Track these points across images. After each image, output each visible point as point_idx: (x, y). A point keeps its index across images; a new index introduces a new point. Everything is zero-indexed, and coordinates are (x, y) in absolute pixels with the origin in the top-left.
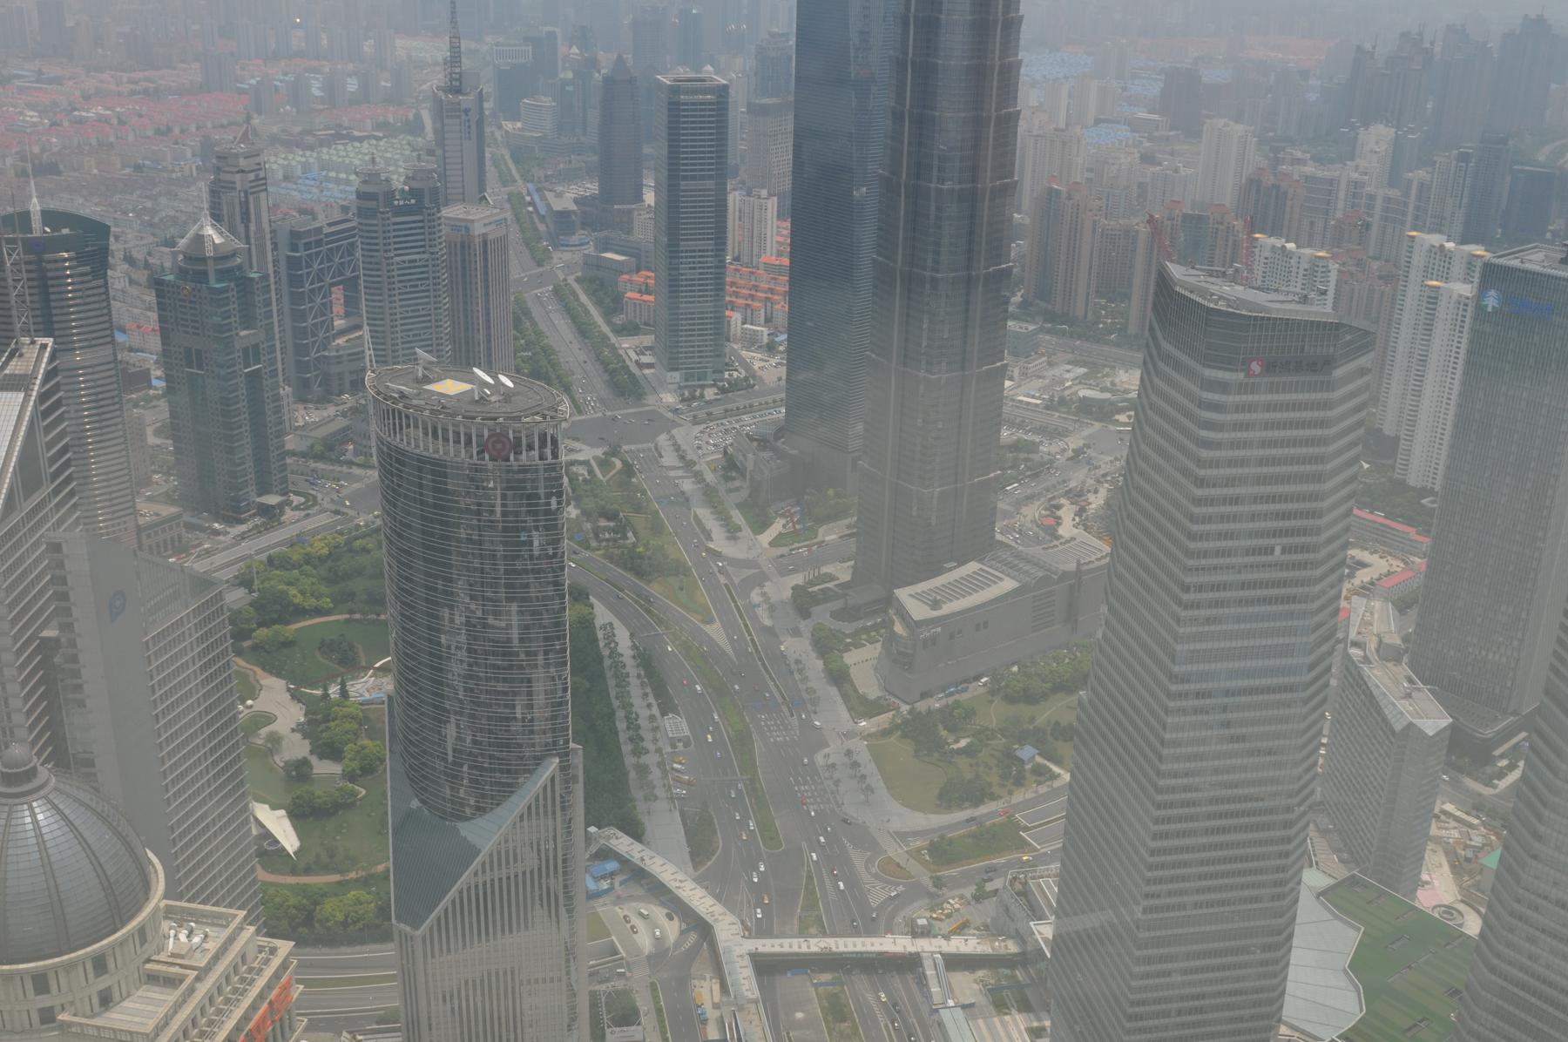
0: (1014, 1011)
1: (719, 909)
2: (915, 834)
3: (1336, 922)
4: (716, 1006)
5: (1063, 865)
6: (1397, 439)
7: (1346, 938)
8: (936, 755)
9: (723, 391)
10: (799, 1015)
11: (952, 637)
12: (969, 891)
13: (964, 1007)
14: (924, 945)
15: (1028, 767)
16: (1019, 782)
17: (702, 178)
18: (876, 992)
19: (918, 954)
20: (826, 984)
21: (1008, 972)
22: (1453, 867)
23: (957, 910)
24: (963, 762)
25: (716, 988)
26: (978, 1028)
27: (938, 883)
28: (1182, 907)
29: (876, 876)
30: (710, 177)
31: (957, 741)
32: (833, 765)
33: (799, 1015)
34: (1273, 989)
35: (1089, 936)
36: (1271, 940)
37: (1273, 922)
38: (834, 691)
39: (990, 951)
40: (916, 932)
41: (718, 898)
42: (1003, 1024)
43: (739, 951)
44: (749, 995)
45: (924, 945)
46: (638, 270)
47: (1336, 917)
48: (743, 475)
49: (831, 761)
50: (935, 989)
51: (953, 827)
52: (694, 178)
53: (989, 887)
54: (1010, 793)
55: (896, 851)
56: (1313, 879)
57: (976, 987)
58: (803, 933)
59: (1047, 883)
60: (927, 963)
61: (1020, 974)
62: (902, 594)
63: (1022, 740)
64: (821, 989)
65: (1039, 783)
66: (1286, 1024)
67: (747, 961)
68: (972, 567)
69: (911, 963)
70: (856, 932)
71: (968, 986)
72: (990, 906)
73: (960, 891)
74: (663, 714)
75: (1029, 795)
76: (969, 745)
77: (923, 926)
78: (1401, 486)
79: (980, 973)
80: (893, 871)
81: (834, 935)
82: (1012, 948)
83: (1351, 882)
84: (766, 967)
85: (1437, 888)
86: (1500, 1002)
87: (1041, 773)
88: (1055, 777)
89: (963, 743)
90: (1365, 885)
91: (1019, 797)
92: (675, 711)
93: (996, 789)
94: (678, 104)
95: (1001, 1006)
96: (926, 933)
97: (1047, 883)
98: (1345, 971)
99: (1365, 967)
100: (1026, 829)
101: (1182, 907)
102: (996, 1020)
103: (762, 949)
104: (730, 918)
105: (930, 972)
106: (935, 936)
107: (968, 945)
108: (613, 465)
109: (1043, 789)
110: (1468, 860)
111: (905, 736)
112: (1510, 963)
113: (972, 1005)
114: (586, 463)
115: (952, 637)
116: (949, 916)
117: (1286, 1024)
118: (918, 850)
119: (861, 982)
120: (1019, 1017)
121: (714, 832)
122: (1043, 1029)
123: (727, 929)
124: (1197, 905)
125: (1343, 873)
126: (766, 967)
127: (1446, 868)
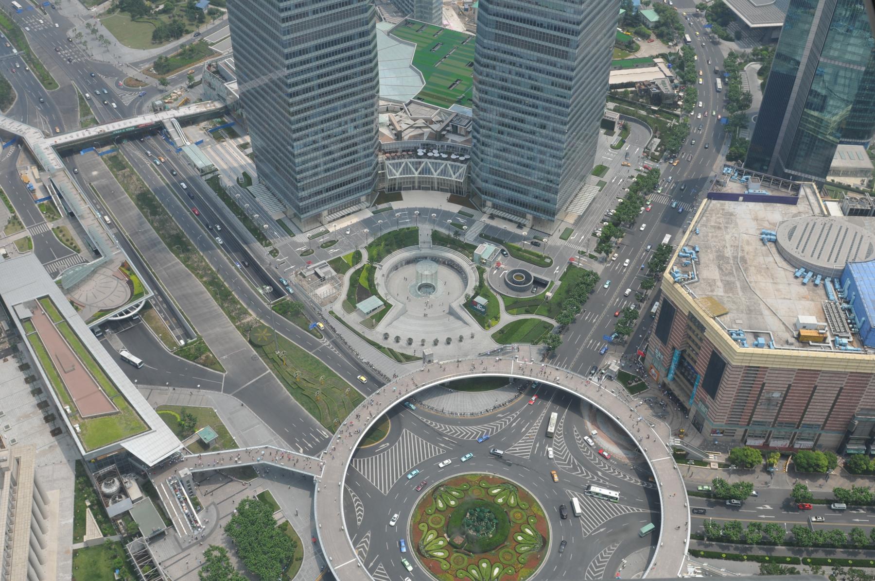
1: (24, 127)
2: (143, 62)
3: (402, 45)
4: (38, 181)
5: (235, 58)
7: (408, 51)
8: (146, 17)
10: (95, 173)
12: (185, 84)
13: (197, 144)
14: (162, 116)
15: (206, 12)
16: (201, 20)
19: (161, 122)
20: (108, 152)
21: (219, 120)
22: (459, 15)
23: (180, 95)
24: (164, 18)
25: (35, 170)
26: (208, 153)
27: (164, 83)
28: (305, 14)
29: (124, 89)
32: (80, 34)
33: (95, 173)
34: (369, 43)
35: (263, 89)
37: (362, 16)
39: (204, 110)
40: (155, 110)
41: (24, 122)
42: (223, 147)
43: (43, 146)
44: (57, 167)
45: (162, 116)
47: (401, 42)
49: (78, 32)
50: (176, 138)
51: (168, 52)
53: (197, 79)
54: (198, 27)
55: (132, 73)
56: (382, 28)
57: (202, 132)
58: (85, 126)
59: (230, 61)
60: (168, 126)
61: (227, 119)
64: (104, 157)
65: (214, 19)
66: (383, 99)
67: (51, 150)
69: (157, 129)
70: (117, 119)
71: (196, 132)
72: (200, 90)
73: (179, 86)
75: (210, 26)
76: (166, 6)
77: (160, 106)
79: (203, 124)
80: (132, 84)
81: (104, 123)
82: (218, 105)
83: (407, 23)
84: (66, 152)
85: (454, 23)
86: (497, 31)
87: (211, 13)
88: (223, 13)
89: (161, 7)
90: (413, 23)
91: (203, 29)
93: (187, 28)
95: (219, 138)
96: (163, 109)
97: (230, 61)
98: (411, 67)
99: (421, 63)
100: (212, 44)
101: (305, 14)
102: (218, 146)
103: (59, 142)
104: (33, 130)
105: (171, 130)
106: (169, 110)
107: (193, 109)
109: (217, 22)
110: (466, 10)
111: (123, 10)
113: (202, 142)
116: (176, 100)
117: (383, 99)
118: (148, 70)
119: (129, 147)
120: (231, 141)
121: (10, 88)
122: (248, 144)
123: (33, 136)
124: (315, 12)
125: (399, 20)
126: (66, 152)
127: (456, 16)
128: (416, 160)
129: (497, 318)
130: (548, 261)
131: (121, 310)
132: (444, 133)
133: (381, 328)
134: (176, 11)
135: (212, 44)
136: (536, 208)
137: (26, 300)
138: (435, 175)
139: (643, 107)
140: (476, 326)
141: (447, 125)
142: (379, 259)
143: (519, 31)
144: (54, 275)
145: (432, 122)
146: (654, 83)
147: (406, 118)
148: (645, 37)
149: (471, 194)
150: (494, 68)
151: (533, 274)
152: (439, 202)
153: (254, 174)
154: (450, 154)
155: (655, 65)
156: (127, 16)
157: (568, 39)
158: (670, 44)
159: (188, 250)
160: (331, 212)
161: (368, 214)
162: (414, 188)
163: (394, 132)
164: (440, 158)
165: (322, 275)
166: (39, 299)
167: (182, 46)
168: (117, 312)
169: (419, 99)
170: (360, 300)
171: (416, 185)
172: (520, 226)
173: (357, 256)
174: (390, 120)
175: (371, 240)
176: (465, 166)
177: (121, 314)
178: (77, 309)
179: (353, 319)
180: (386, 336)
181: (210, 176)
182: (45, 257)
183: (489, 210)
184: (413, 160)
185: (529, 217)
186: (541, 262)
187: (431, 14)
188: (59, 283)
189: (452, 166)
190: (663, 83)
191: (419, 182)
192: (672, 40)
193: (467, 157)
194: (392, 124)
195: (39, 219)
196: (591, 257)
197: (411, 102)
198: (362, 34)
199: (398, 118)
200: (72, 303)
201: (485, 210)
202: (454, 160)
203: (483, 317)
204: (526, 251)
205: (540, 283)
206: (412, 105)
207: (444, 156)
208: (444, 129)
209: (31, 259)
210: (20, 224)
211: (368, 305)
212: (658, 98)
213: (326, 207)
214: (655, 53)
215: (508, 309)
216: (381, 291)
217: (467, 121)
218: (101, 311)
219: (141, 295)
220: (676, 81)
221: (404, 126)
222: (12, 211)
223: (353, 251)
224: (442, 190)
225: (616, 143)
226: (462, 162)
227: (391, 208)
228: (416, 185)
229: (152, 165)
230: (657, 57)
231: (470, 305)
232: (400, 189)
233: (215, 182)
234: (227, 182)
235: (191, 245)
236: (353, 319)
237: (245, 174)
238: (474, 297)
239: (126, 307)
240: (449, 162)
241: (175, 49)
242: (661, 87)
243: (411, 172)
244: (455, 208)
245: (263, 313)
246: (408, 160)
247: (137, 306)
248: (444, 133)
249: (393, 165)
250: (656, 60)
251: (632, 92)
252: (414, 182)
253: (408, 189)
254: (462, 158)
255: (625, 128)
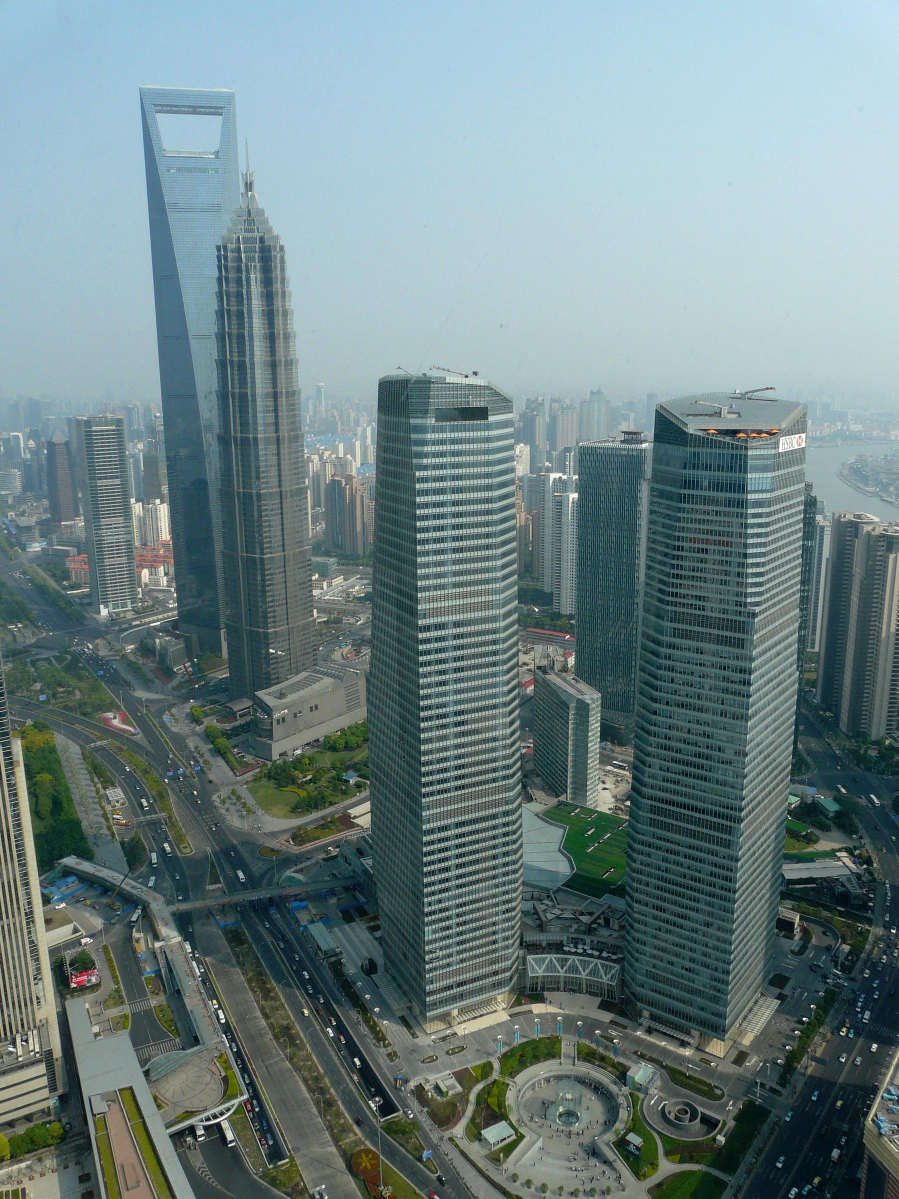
0: (358, 920)
3: (552, 827)
6: (552, 594)
9: (137, 612)
11: (295, 716)
17: (112, 478)
18: (262, 922)
26: (335, 934)
30: (117, 477)
31: (305, 777)
36: (508, 808)
38: (220, 762)
46: (79, 554)
47: (551, 824)
48: (155, 655)
51: (308, 824)
52: (105, 478)
62: (260, 694)
63: (347, 768)
68: (304, 674)
74: (105, 788)
76: (314, 777)
78: (559, 616)
89: (309, 777)
92: (113, 785)
94: (91, 431)
95: (348, 918)
98: (560, 850)
102: (346, 927)
108: (66, 658)
112: (652, 787)
114: (47, 660)
115: (295, 716)
125: (553, 801)
128: (562, 956)
129: (654, 1165)
130: (718, 1092)
131: (209, 1113)
132: (594, 926)
133: (509, 1165)
134: (323, 782)
135: (355, 817)
136: (703, 1023)
137: (105, 1090)
138: (584, 975)
139: (826, 908)
140: (627, 1174)
141: (599, 917)
142: (513, 1074)
143: (676, 816)
144: (143, 1062)
145: (582, 914)
146: (838, 879)
147: (554, 907)
148: (825, 828)
149: (626, 1002)
150: (649, 855)
151: (700, 1109)
152: (587, 1008)
153: (380, 961)
154: (601, 951)
155: (839, 859)
156: (272, 784)
157: (730, 827)
158: (854, 836)
159: (295, 1045)
160: (462, 1011)
161: (503, 1017)
162: (558, 990)
163: (538, 922)
164: (591, 956)
165: (444, 1089)
166: (120, 1090)
167: (323, 818)
168: (203, 1116)
169: (568, 886)
170: (487, 1125)
171: (562, 986)
172: (684, 1044)
173: (487, 1068)
174: (534, 908)
175: (505, 1049)
176: (618, 966)
177: (208, 1119)
178: (159, 1107)
179: (475, 1150)
180: (514, 1178)
181: (333, 959)
182: (137, 1041)
183: (646, 1022)
184: (558, 956)
185: (695, 1033)
186: (709, 1093)
187: (586, 796)
188: (147, 1073)
189: (603, 966)
190: (849, 880)
191: (565, 983)
192: (856, 833)
193: (620, 956)
194: (536, 913)
195: (143, 994)
196: (772, 1090)
197: (559, 890)
198: (506, 814)
199: (543, 907)
200: (155, 1098)
201: (640, 1021)
202: (606, 959)
203: (638, 1162)
204: (690, 1077)
205: (710, 1124)
206: (561, 894)
207: (596, 953)
208: (594, 922)
209: (123, 1039)
210: (121, 997)
211: (495, 1133)
212: (844, 898)
213: (455, 1005)
214: (837, 846)
215: (667, 1154)
216: (513, 1118)
217: (621, 914)
218: (187, 1112)
219: (235, 1096)
220: (864, 879)
221: (550, 916)
222: (117, 983)
223: (483, 1061)
224: (591, 993)
225: (797, 949)
226: (614, 961)
227: (530, 1012)
228: (562, 986)
229: (272, 942)
230: (840, 850)
231: (621, 1144)
232: (543, 989)
233: (337, 967)
234: (351, 969)
235: (301, 1040)
236: (475, 1150)
237: (371, 961)
238: (626, 1134)
239: (216, 1110)
240: (599, 961)
241: (317, 820)
242: (847, 884)
243: (556, 970)
244: (606, 1017)
245: (371, 1134)
246: (553, 956)
247: (228, 1110)
248: (594, 926)
249: (535, 960)
250: (838, 854)
251: (813, 889)
252: (559, 982)
253: (553, 990)
254: (614, 957)
255: (806, 933)
